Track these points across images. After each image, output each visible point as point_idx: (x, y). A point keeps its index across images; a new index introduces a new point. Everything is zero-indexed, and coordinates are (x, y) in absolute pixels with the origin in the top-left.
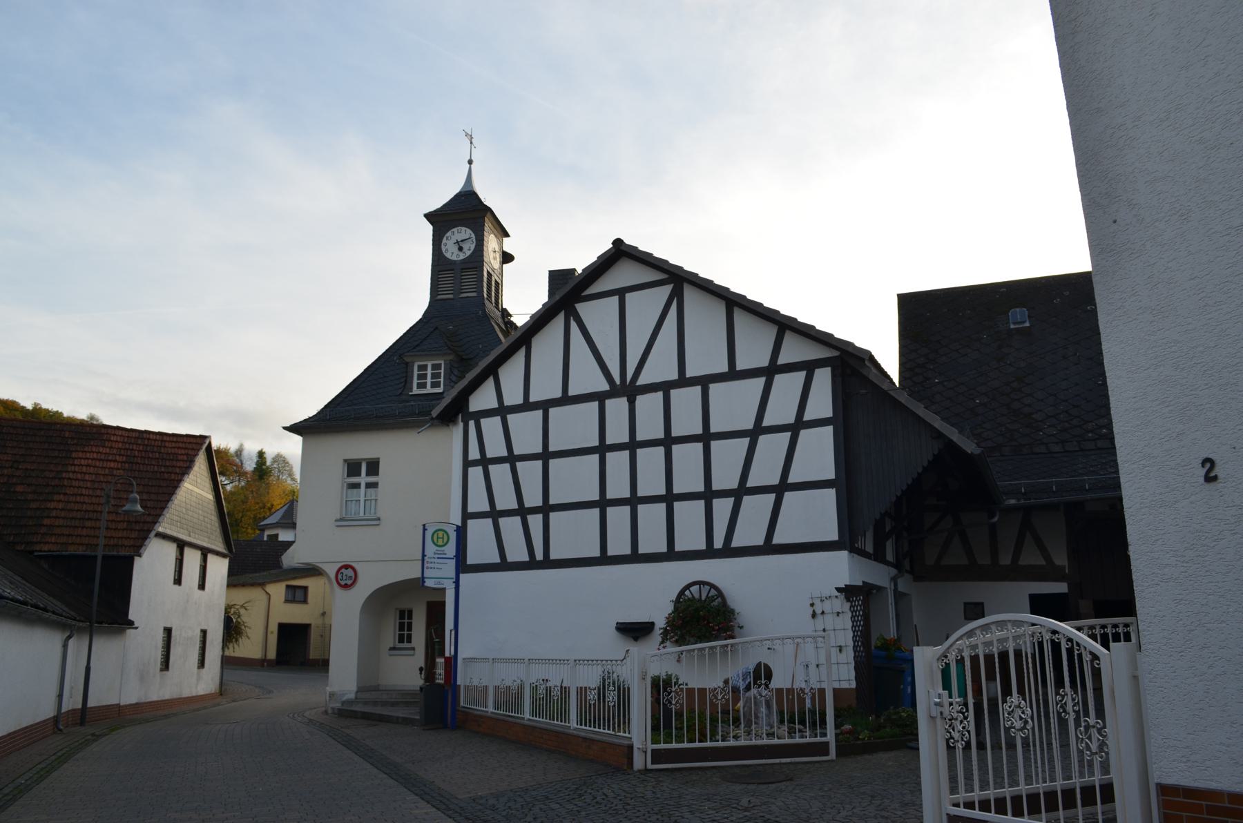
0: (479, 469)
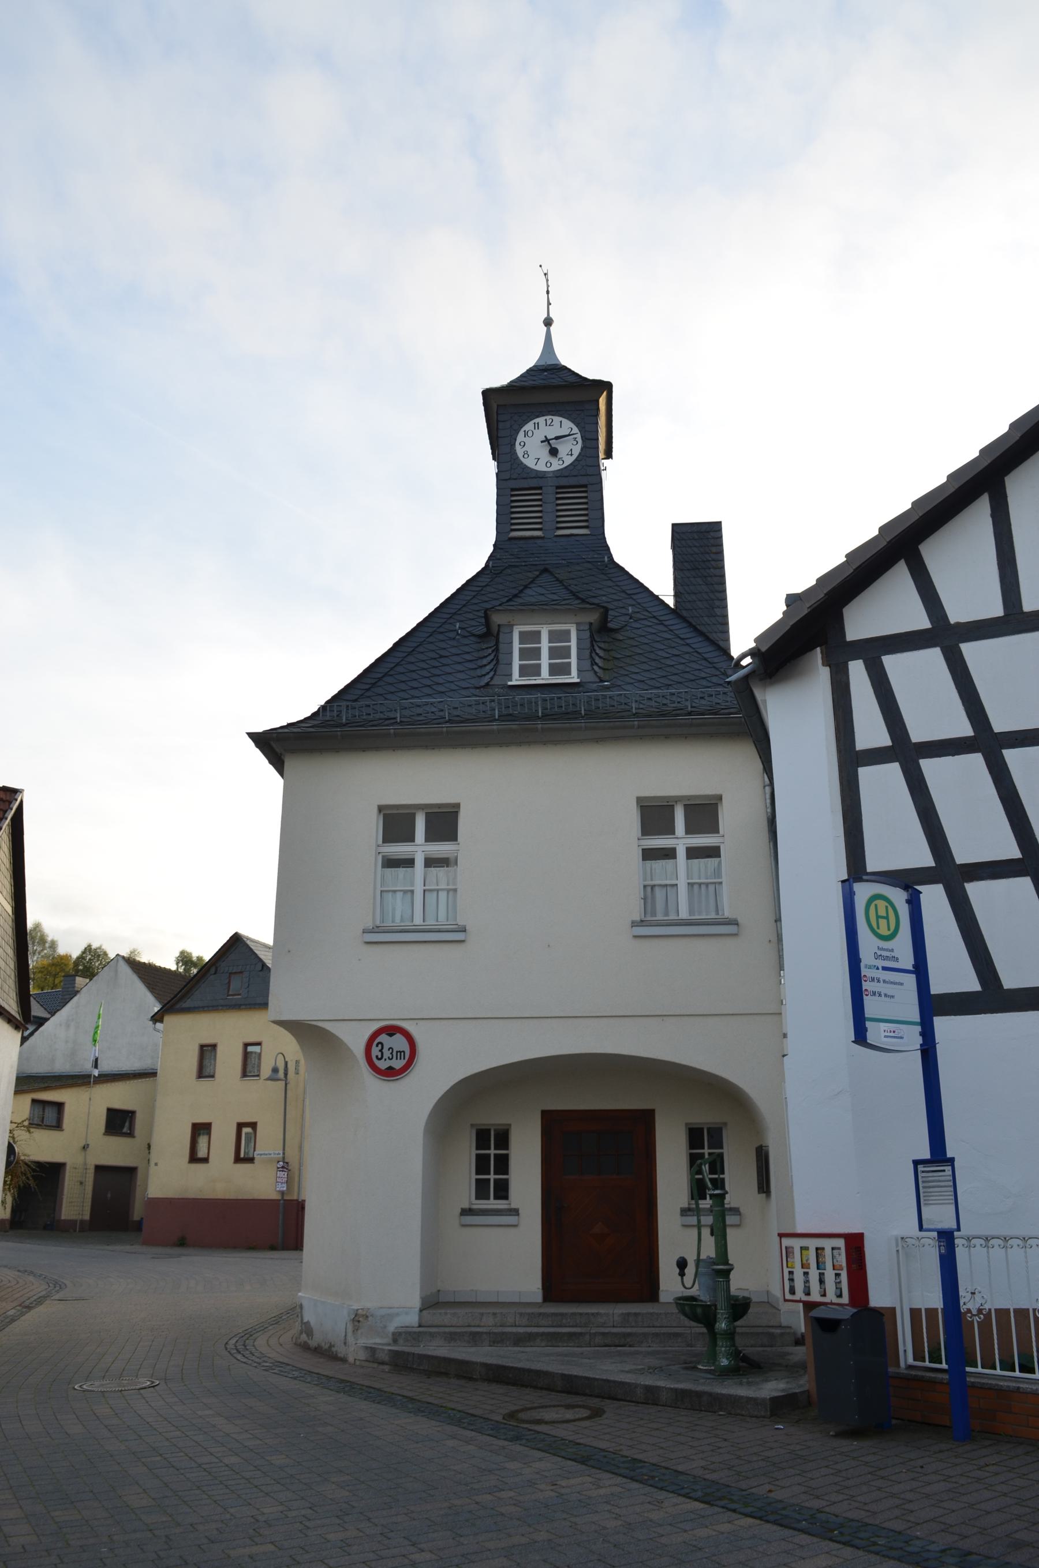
0: (893, 771)
